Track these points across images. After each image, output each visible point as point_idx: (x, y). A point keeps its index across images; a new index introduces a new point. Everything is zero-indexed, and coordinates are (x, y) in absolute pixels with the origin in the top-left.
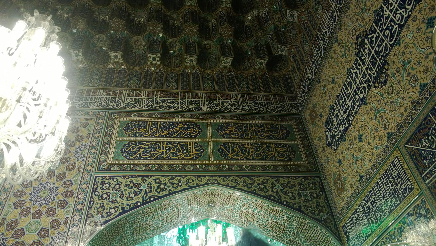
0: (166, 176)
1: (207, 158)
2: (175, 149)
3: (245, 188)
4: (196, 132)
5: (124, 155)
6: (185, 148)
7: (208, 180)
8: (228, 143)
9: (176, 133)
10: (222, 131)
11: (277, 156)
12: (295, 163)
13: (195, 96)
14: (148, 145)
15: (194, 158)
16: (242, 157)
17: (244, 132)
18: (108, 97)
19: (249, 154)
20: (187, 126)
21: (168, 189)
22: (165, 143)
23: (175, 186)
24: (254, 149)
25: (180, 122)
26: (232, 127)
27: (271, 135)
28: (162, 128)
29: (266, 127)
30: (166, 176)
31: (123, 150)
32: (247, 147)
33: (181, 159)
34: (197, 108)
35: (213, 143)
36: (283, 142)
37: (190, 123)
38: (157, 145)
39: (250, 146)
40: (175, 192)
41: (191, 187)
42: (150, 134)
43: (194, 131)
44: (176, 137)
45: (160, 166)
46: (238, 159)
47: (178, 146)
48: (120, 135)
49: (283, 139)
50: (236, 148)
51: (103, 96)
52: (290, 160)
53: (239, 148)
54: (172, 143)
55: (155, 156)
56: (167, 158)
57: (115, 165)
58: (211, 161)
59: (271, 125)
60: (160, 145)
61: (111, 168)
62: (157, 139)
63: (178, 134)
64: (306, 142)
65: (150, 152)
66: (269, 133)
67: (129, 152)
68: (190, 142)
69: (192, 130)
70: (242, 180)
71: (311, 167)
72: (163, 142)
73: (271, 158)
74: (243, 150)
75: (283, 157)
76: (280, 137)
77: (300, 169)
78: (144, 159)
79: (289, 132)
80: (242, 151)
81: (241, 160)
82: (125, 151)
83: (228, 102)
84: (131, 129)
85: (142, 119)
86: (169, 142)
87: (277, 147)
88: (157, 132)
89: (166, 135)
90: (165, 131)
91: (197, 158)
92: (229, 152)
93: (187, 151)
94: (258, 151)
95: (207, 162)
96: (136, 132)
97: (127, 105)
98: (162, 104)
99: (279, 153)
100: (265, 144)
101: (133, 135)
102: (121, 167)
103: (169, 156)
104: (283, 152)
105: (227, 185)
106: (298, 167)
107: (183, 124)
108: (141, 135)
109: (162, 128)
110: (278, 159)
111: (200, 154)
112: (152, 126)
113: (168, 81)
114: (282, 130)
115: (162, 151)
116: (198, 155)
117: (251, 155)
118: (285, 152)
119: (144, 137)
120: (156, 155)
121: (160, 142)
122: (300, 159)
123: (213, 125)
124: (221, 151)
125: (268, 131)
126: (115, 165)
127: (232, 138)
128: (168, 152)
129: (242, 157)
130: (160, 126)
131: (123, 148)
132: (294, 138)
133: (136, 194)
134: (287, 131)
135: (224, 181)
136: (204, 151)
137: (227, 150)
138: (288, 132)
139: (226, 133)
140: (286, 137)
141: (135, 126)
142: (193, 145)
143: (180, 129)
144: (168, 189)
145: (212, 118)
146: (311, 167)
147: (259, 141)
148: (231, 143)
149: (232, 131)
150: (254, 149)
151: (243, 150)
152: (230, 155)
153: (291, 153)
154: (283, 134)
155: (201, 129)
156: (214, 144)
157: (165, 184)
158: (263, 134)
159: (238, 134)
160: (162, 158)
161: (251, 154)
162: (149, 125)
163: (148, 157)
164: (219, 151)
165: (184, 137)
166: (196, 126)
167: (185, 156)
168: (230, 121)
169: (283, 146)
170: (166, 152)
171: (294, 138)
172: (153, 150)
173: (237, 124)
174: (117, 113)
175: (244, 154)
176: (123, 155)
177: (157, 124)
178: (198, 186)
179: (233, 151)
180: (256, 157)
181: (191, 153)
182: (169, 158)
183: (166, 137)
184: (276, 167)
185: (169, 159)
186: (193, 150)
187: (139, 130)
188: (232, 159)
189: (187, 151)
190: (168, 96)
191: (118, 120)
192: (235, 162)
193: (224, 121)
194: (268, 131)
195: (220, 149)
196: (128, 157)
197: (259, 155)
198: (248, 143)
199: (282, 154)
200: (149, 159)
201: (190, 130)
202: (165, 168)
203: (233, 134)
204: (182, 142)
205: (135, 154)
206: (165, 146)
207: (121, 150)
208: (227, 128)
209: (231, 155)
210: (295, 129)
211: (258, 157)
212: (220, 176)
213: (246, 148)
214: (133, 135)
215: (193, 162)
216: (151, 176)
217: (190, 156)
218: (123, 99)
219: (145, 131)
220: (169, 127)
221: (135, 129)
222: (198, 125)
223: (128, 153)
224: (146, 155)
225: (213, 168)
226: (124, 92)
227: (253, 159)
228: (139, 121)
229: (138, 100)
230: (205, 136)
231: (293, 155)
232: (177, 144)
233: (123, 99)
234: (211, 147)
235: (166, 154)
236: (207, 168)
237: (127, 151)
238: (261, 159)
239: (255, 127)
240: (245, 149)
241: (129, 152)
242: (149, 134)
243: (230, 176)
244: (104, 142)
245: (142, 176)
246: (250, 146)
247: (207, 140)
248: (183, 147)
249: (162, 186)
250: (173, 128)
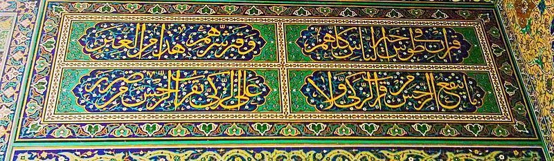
2: (202, 86)
4: (249, 47)
5: (83, 102)
6: (223, 85)
8: (326, 72)
9: (204, 49)
10: (310, 45)
11: (438, 102)
12: (483, 117)
14: (139, 77)
15: (247, 107)
16: (359, 105)
17: (361, 47)
19: (375, 98)
20: (230, 33)
22: (178, 72)
24: (386, 85)
26: (333, 34)
27: (425, 53)
28: (170, 39)
29: (415, 34)
31: (80, 90)
32: (369, 80)
33: (216, 110)
35: (291, 72)
36: (454, 68)
38: (159, 77)
39: (376, 80)
42: (143, 53)
43: (246, 45)
44: (203, 59)
47: (209, 79)
48: (70, 55)
49: (454, 62)
50: (344, 82)
52: (471, 109)
53: (352, 84)
54: (195, 72)
55: (154, 103)
56: (183, 108)
57: (60, 125)
58: (286, 114)
59: (424, 29)
60: (165, 77)
61: (51, 132)
62: (158, 65)
63: (209, 53)
64: (506, 68)
65: (142, 93)
66: (420, 49)
67: (94, 95)
69: (242, 41)
71: (520, 127)
72: (174, 71)
73: (425, 106)
74: (361, 89)
75: (455, 104)
76: (447, 57)
77: (494, 132)
78: (129, 110)
79: (468, 46)
80: (358, 91)
81: (356, 111)
82: (84, 92)
84: (98, 41)
86: (186, 71)
87: (440, 81)
88: (158, 48)
89: (180, 55)
90: (179, 46)
91: (252, 107)
92: (327, 92)
93: (228, 92)
94: (396, 91)
95: (277, 117)
96: (110, 48)
99: (444, 94)
100: (413, 73)
101: (102, 56)
102: (74, 129)
103: (188, 104)
104: (453, 91)
106: (489, 127)
107: (219, 29)
108: (122, 55)
109: (170, 39)
110: (441, 108)
111: (259, 99)
112: (146, 34)
114: (450, 40)
115: (170, 91)
116: (256, 101)
117: (378, 99)
118: (458, 91)
119: (128, 58)
120: (157, 100)
121: (166, 71)
122: (493, 108)
123: (289, 30)
124: (308, 90)
125: (419, 43)
126: (60, 125)
128: (184, 93)
129: (359, 105)
130: (166, 34)
131: (79, 86)
132: (479, 59)
134: (463, 42)
136: (268, 90)
137: (322, 89)
138: (465, 46)
139: (319, 50)
140: (460, 57)
141: (104, 33)
142: (242, 77)
146: (520, 127)
147: (398, 68)
148: (333, 72)
149: (335, 44)
150: (386, 85)
151: (361, 89)
152: (329, 101)
153: (475, 94)
154: (453, 51)
155: (261, 39)
158: (406, 51)
159: (349, 52)
161: (379, 97)
162: (140, 30)
163: (139, 107)
164: (303, 90)
165: (222, 59)
166: (250, 33)
167: (224, 103)
169: (454, 79)
170: (179, 93)
171: (479, 59)
172: (149, 90)
175: (363, 97)
176: (79, 102)
177: (159, 29)
179: (338, 90)
180: (391, 104)
181: (239, 97)
182: (188, 107)
183: (180, 58)
184: (437, 126)
185: (186, 110)
186: (242, 89)
187: (117, 43)
189: (228, 92)
194: (417, 44)
196: (91, 107)
197: (399, 100)
198: (372, 72)
199: (450, 98)
200: (140, 109)
201: (235, 43)
202: (179, 131)
203: (338, 51)
205: (108, 98)
206: (177, 80)
208: (322, 37)
209: (332, 101)
210: (482, 39)
211: (396, 103)
213: (367, 82)
214: (102, 56)
217: (236, 103)
220: (187, 35)
221: (106, 41)
222: (255, 31)
223: (91, 98)
224: (134, 102)
227: (384, 109)
231: (477, 98)
232: (207, 75)
234: (284, 82)
235: (181, 99)
236: (275, 129)
237: (91, 91)
238: (403, 109)
239: (387, 34)
240: (364, 85)
241: (94, 95)
242: (140, 53)
244: (34, 71)
246: (376, 80)
247: (275, 66)
248: (220, 82)
250: (195, 39)
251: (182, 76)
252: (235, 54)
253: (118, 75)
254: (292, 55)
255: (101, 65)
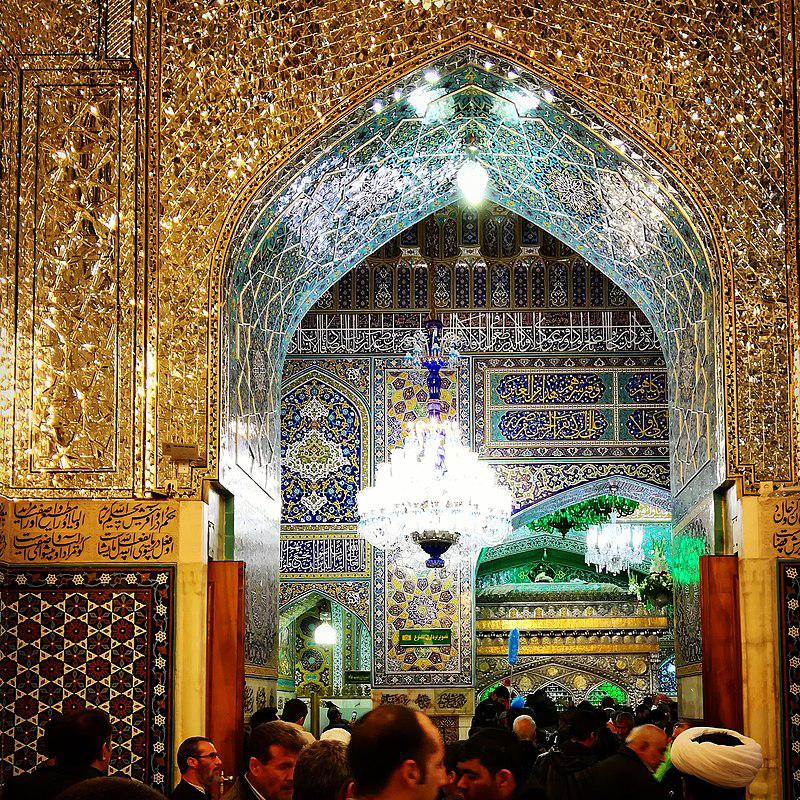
0: (560, 465)
1: (610, 437)
3: (658, 481)
7: (612, 470)
8: (641, 410)
13: (596, 319)
18: (467, 328)
20: (586, 381)
21: (562, 482)
23: (571, 478)
25: (574, 375)
26: (648, 381)
28: (548, 387)
30: (560, 465)
34: (597, 345)
37: (587, 375)
40: (571, 487)
41: (591, 480)
45: (551, 450)
46: (652, 438)
51: (460, 327)
68: (588, 411)
69: (591, 388)
70: (654, 469)
72: (552, 411)
80: (660, 425)
83: (646, 329)
85: (520, 371)
90: (554, 393)
92: (641, 426)
95: (611, 443)
96: (515, 395)
97: (498, 344)
98: (545, 340)
105: (636, 477)
109: (548, 387)
113: (552, 288)
119: (526, 403)
127: (649, 402)
130: (546, 384)
133: (526, 490)
135: (631, 471)
141: (511, 383)
143: (574, 386)
144: (562, 482)
145: (621, 364)
148: (646, 410)
156: (623, 414)
157: (558, 476)
160: (551, 438)
164: (627, 424)
165: (580, 402)
168: (646, 370)
173: (657, 374)
174: (484, 361)
175: (662, 429)
178: (598, 477)
183: (556, 402)
188: (645, 438)
190: (554, 320)
191: (489, 373)
192: (648, 443)
193: (638, 370)
195: (629, 422)
202: (557, 453)
204: (577, 411)
205: (518, 431)
206: (555, 418)
207: (500, 426)
212: (626, 464)
215: (593, 443)
216: (541, 465)
218: (488, 332)
219: (526, 392)
225: (618, 453)
226: (488, 316)
228: (516, 376)
229: (511, 333)
230: (608, 400)
233: (488, 332)
234: (616, 416)
243: (639, 464)
245: (530, 465)
249: (555, 479)
250: (564, 386)
251: (557, 416)
252: (588, 398)
253: (522, 416)
254: (623, 399)
255: (512, 408)
